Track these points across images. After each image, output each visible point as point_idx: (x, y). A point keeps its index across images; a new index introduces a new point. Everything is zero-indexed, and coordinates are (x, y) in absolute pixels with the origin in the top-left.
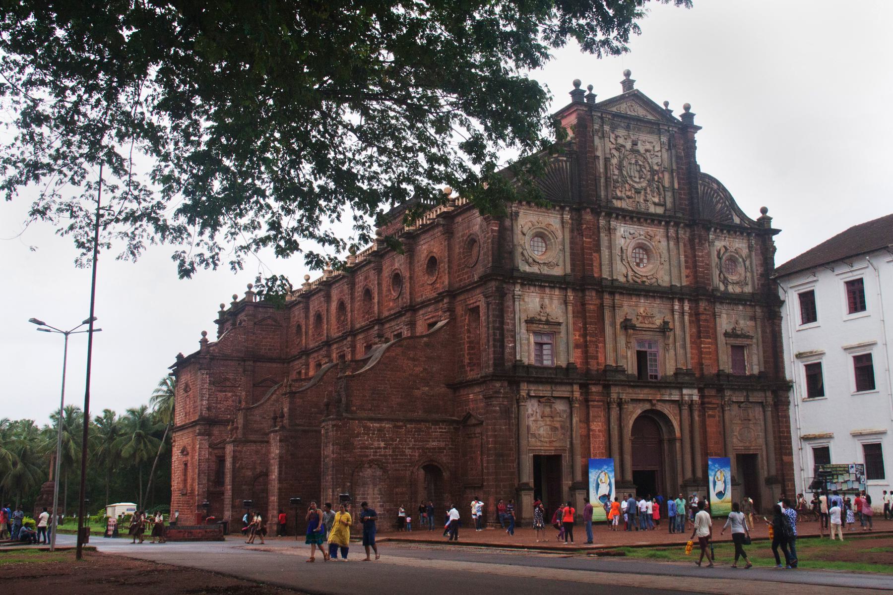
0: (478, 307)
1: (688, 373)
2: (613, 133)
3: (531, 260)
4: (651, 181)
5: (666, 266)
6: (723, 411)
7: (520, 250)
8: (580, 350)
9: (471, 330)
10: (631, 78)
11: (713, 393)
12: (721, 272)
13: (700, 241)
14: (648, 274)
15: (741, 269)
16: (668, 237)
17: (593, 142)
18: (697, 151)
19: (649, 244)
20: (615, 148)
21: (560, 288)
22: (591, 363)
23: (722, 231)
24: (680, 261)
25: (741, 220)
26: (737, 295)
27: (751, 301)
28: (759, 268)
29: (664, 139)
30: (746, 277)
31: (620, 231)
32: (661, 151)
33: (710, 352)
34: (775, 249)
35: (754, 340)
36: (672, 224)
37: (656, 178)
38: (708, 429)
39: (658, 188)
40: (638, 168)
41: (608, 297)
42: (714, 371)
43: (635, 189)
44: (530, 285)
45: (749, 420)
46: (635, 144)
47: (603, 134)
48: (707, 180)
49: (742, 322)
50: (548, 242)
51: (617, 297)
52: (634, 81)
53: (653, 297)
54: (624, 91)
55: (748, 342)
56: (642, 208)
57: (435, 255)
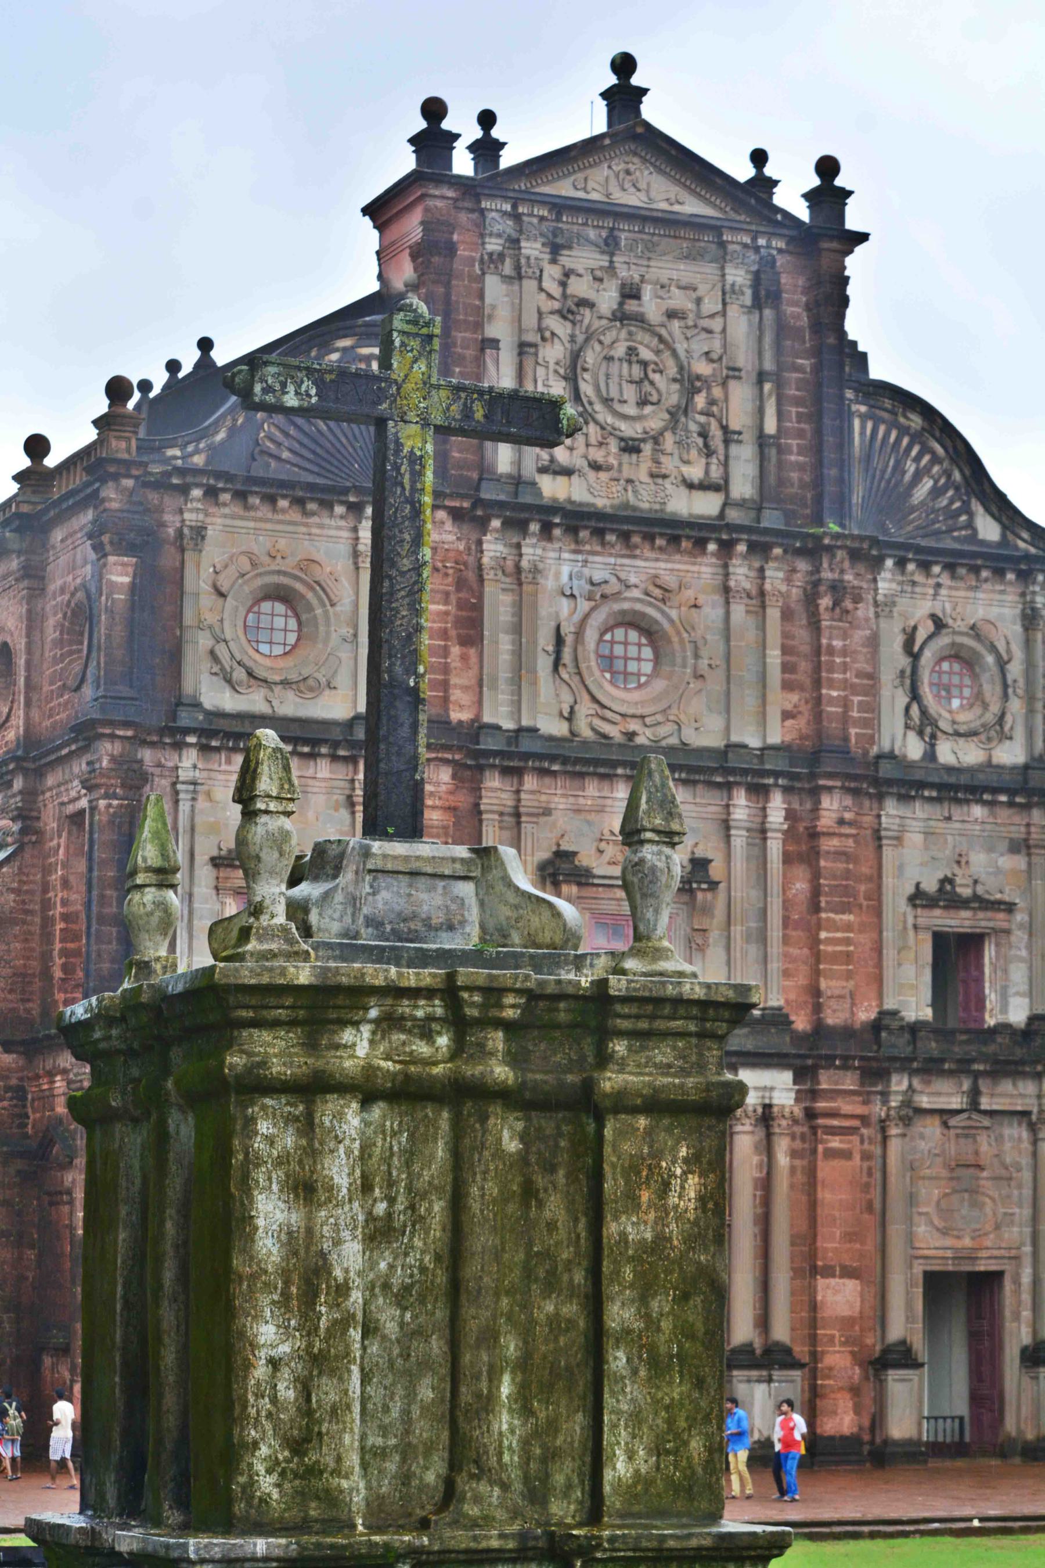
0: (84, 810)
2: (554, 261)
3: (240, 674)
4: (677, 415)
5: (715, 683)
6: (885, 1139)
7: (204, 641)
9: (72, 879)
10: (636, 80)
11: (849, 1082)
12: (915, 696)
13: (836, 603)
14: (645, 711)
16: (726, 590)
17: (481, 296)
18: (849, 312)
21: (334, 758)
24: (764, 664)
25: (1004, 528)
26: (971, 770)
27: (1012, 792)
29: (738, 276)
31: (558, 575)
32: (724, 313)
33: (848, 957)
35: (1020, 917)
36: (742, 548)
37: (700, 401)
38: (825, 1195)
39: (704, 434)
40: (637, 371)
42: (865, 1014)
43: (622, 439)
44: (235, 750)
45: (979, 1167)
46: (630, 292)
47: (518, 268)
48: (888, 404)
49: (979, 861)
50: (304, 617)
51: (530, 782)
52: (644, 91)
54: (610, 124)
56: (644, 500)
57: (9, 640)
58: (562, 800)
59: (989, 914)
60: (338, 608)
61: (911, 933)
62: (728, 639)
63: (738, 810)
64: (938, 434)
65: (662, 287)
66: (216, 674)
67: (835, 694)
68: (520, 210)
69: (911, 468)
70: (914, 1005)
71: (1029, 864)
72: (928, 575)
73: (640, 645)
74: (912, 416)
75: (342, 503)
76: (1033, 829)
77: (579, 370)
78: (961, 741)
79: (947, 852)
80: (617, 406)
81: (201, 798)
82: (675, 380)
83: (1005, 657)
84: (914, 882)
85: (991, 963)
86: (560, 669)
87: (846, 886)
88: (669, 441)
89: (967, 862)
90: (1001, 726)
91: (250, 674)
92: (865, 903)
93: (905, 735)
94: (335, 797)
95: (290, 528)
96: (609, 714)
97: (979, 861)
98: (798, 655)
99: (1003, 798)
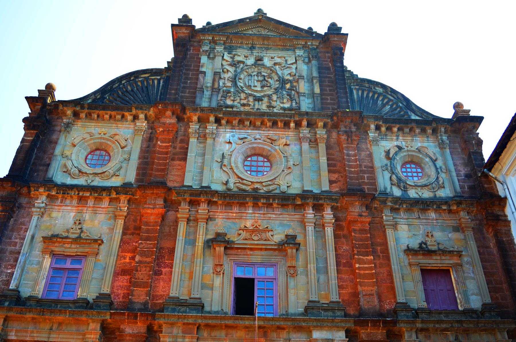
1: (331, 307)
8: (127, 277)
15: (432, 172)
16: (300, 140)
19: (269, 148)
20: (230, 65)
22: (135, 293)
23: (389, 129)
28: (462, 169)
29: (299, 52)
30: (438, 178)
34: (480, 142)
35: (466, 259)
36: (305, 123)
37: (288, 86)
40: (260, 78)
41: (187, 207)
48: (367, 85)
49: (439, 235)
53: (269, 206)
55: (455, 260)
58: (220, 214)
59: (448, 257)
60: (125, 149)
61: (408, 268)
62: (301, 155)
63: (308, 215)
64: (390, 93)
65: (272, 58)
66: (64, 172)
67: (353, 170)
68: (215, 39)
69: (380, 103)
70: (416, 300)
71: (465, 236)
72: (392, 133)
73: (264, 162)
74: (377, 88)
75: (131, 115)
76: (462, 220)
77: (237, 79)
78: (419, 189)
79: (421, 232)
80: (252, 88)
81: (45, 216)
82: (277, 81)
83: (434, 158)
84: (406, 245)
85: (455, 280)
86: (223, 167)
87: (367, 244)
88: (275, 97)
89: (432, 236)
90: (438, 183)
91: (80, 171)
92: (381, 255)
93: (391, 187)
94: (110, 215)
95: (109, 125)
96: (245, 182)
97: (439, 235)
98: (336, 161)
99: (444, 207)
